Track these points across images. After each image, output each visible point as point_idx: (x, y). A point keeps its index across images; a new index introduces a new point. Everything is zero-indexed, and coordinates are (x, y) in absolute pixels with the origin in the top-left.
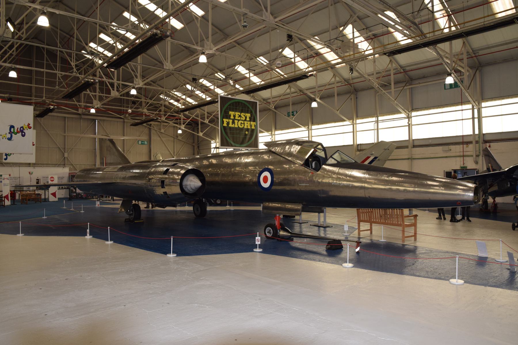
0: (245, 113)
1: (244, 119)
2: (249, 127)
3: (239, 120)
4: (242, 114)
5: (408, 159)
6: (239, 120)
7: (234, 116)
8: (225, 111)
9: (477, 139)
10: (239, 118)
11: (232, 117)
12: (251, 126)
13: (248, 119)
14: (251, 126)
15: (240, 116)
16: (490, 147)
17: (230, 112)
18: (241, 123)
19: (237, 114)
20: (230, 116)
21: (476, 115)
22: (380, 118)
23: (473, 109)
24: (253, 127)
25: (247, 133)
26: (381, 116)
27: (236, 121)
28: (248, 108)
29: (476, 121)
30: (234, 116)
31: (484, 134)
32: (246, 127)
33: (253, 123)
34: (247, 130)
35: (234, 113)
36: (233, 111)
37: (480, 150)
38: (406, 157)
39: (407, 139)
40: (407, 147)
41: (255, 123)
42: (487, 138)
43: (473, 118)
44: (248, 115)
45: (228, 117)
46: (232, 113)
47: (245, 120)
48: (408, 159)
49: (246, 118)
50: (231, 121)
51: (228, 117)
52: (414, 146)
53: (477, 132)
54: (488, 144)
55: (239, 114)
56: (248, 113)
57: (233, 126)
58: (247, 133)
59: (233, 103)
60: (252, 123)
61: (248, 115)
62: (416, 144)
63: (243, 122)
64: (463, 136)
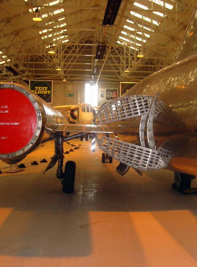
0: (44, 86)
1: (44, 89)
2: (46, 93)
3: (40, 91)
4: (42, 88)
6: (40, 91)
7: (38, 89)
8: (33, 87)
10: (41, 89)
11: (37, 89)
12: (47, 93)
13: (46, 89)
14: (47, 93)
15: (41, 88)
17: (36, 87)
18: (42, 92)
19: (39, 88)
20: (36, 89)
24: (49, 93)
25: (45, 96)
27: (39, 91)
28: (46, 84)
30: (38, 89)
32: (44, 93)
33: (49, 92)
34: (45, 94)
35: (38, 87)
36: (37, 86)
41: (50, 91)
44: (46, 88)
45: (35, 89)
46: (36, 88)
47: (44, 90)
49: (45, 89)
50: (36, 91)
51: (35, 89)
55: (41, 87)
56: (46, 86)
57: (37, 93)
58: (45, 96)
59: (37, 83)
60: (48, 91)
61: (46, 88)
63: (43, 91)
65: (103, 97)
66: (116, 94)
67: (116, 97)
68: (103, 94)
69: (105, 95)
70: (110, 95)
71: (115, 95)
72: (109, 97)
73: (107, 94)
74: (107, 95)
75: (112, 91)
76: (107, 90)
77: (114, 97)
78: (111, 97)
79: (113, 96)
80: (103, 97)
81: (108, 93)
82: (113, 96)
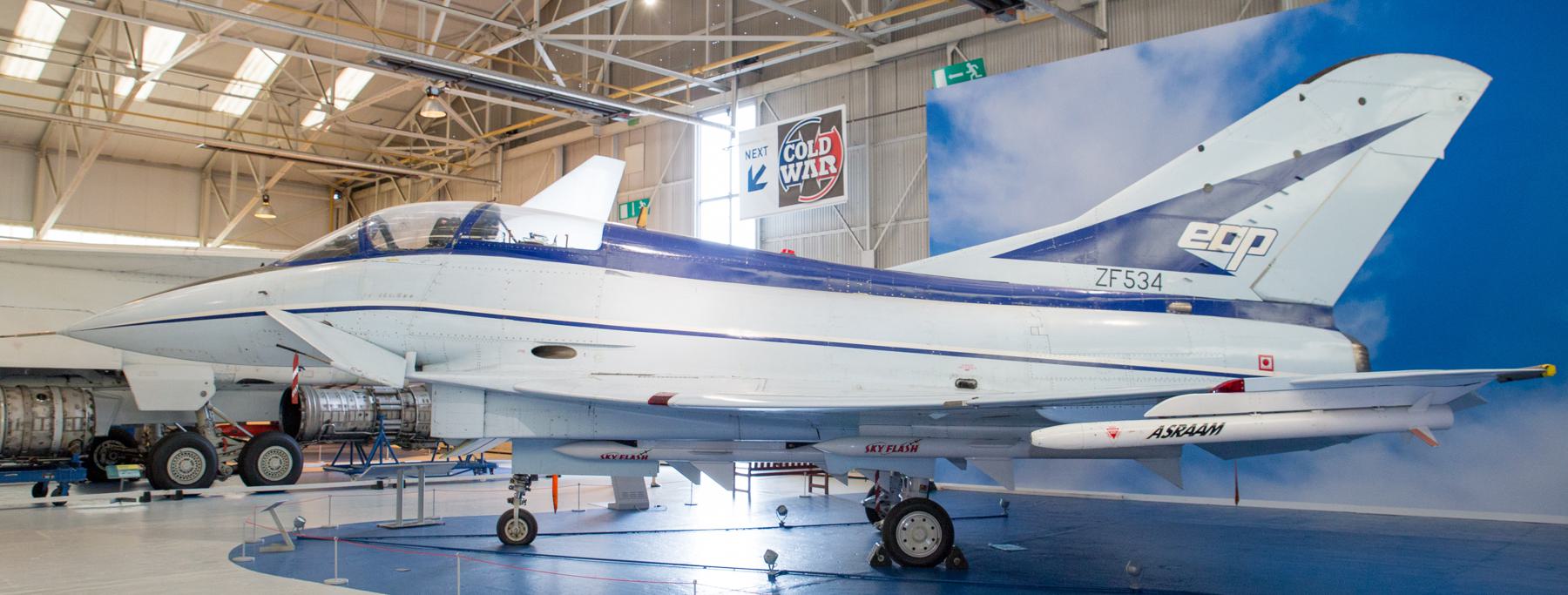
65: (763, 185)
66: (835, 150)
67: (833, 170)
68: (763, 168)
69: (771, 178)
70: (799, 165)
71: (831, 160)
72: (796, 179)
73: (783, 162)
74: (784, 168)
75: (809, 131)
76: (783, 130)
77: (823, 172)
78: (806, 176)
79: (818, 165)
80: (763, 185)
81: (791, 152)
82: (818, 165)
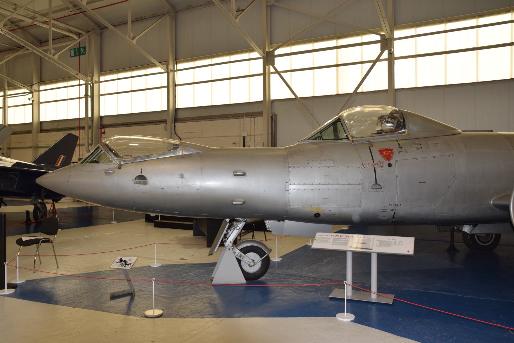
5: (31, 147)
9: (90, 124)
16: (104, 133)
21: (89, 94)
22: (9, 93)
23: (87, 85)
26: (9, 90)
29: (89, 99)
31: (101, 118)
37: (92, 137)
38: (29, 145)
39: (31, 122)
40: (29, 132)
42: (105, 122)
43: (86, 96)
48: (31, 147)
52: (42, 131)
53: (90, 115)
54: (103, 130)
62: (45, 127)
64: (79, 119)
